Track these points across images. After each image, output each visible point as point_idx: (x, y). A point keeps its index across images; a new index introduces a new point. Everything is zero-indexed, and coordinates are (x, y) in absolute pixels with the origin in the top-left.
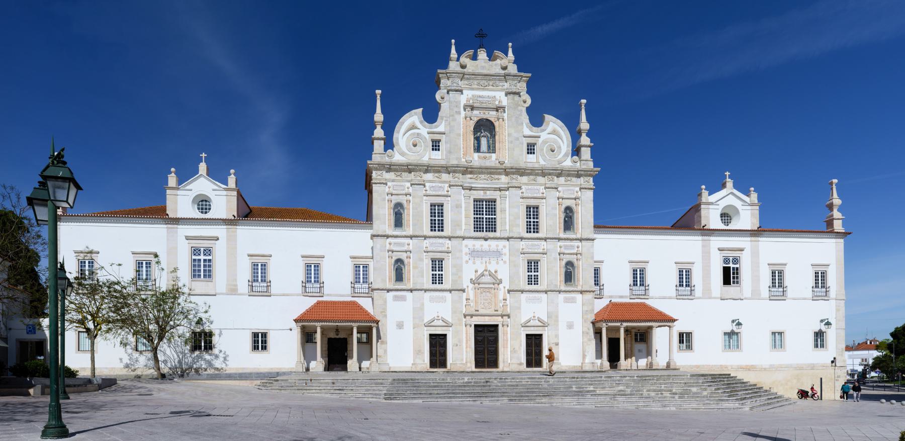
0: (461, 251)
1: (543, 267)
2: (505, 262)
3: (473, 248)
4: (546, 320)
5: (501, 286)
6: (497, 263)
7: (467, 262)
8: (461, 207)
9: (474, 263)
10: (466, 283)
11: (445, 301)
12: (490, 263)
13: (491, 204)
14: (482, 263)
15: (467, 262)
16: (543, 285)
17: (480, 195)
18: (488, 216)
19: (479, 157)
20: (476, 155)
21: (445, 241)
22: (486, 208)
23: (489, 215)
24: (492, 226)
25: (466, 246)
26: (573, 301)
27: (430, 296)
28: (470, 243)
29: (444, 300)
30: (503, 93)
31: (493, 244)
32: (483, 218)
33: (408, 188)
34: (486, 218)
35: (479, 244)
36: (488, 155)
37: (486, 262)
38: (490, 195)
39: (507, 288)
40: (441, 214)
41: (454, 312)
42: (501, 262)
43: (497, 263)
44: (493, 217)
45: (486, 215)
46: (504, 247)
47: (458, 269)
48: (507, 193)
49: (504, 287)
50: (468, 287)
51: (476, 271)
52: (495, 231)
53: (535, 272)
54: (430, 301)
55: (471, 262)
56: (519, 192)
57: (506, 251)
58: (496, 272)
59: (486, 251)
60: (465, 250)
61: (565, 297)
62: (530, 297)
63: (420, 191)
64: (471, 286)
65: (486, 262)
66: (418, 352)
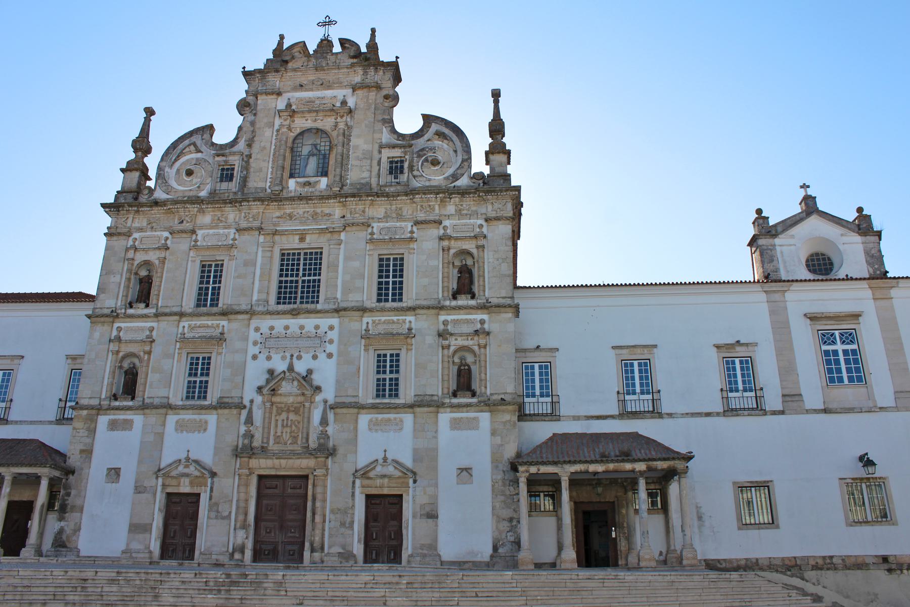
0: (246, 339)
1: (408, 362)
2: (330, 356)
3: (270, 332)
4: (409, 463)
5: (319, 398)
6: (315, 357)
7: (255, 357)
8: (254, 265)
9: (269, 358)
10: (249, 394)
11: (205, 430)
12: (299, 358)
13: (314, 260)
14: (284, 358)
15: (255, 357)
16: (407, 394)
17: (293, 243)
18: (307, 278)
19: (297, 182)
20: (292, 183)
21: (218, 322)
22: (305, 264)
23: (310, 275)
24: (312, 291)
25: (257, 329)
26: (473, 424)
27: (177, 422)
28: (265, 323)
29: (202, 427)
30: (351, 90)
31: (309, 323)
32: (297, 282)
33: (167, 238)
34: (304, 281)
35: (279, 323)
36: (312, 180)
37: (292, 356)
38: (312, 241)
39: (331, 400)
40: (218, 278)
41: (217, 451)
42: (322, 356)
43: (315, 357)
44: (317, 278)
45: (304, 275)
46: (331, 328)
47: (240, 370)
48: (343, 236)
49: (325, 402)
50: (252, 401)
51: (271, 372)
52: (318, 302)
53: (391, 372)
54: (176, 430)
55: (262, 357)
56: (363, 235)
57: (334, 335)
58: (310, 372)
59: (293, 337)
60: (253, 336)
61: (455, 419)
62: (377, 419)
63: (181, 245)
64: (259, 399)
65: (292, 356)
66: (138, 528)
